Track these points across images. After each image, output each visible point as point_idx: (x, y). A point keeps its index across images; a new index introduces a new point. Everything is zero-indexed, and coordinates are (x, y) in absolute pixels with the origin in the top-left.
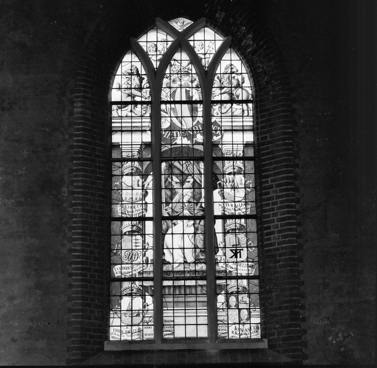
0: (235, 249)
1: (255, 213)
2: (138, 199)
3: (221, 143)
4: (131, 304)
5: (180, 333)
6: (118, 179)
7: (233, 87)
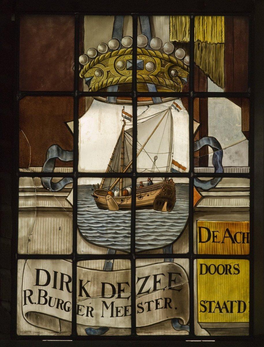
4: (129, 139)
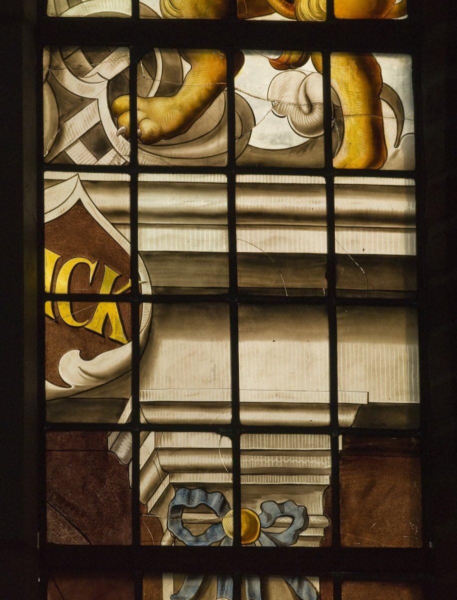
3: (125, 417)
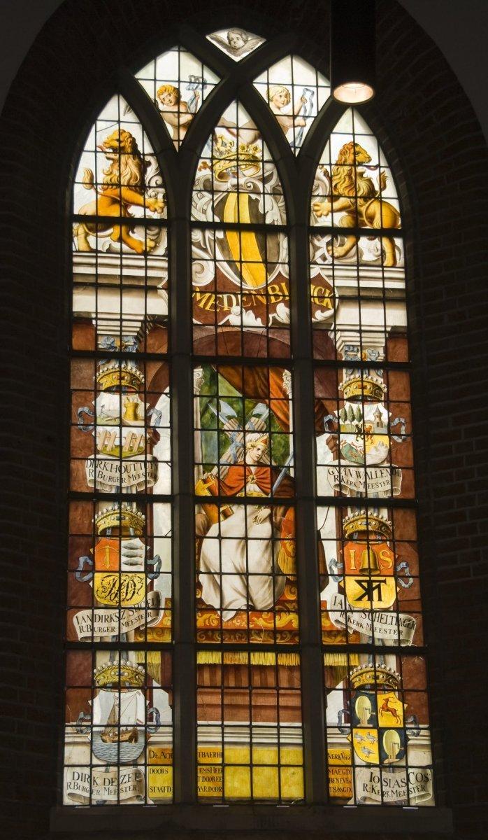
0: (368, 578)
1: (411, 495)
2: (135, 450)
3: (332, 328)
4: (117, 709)
5: (237, 785)
6: (86, 399)
7: (360, 197)
